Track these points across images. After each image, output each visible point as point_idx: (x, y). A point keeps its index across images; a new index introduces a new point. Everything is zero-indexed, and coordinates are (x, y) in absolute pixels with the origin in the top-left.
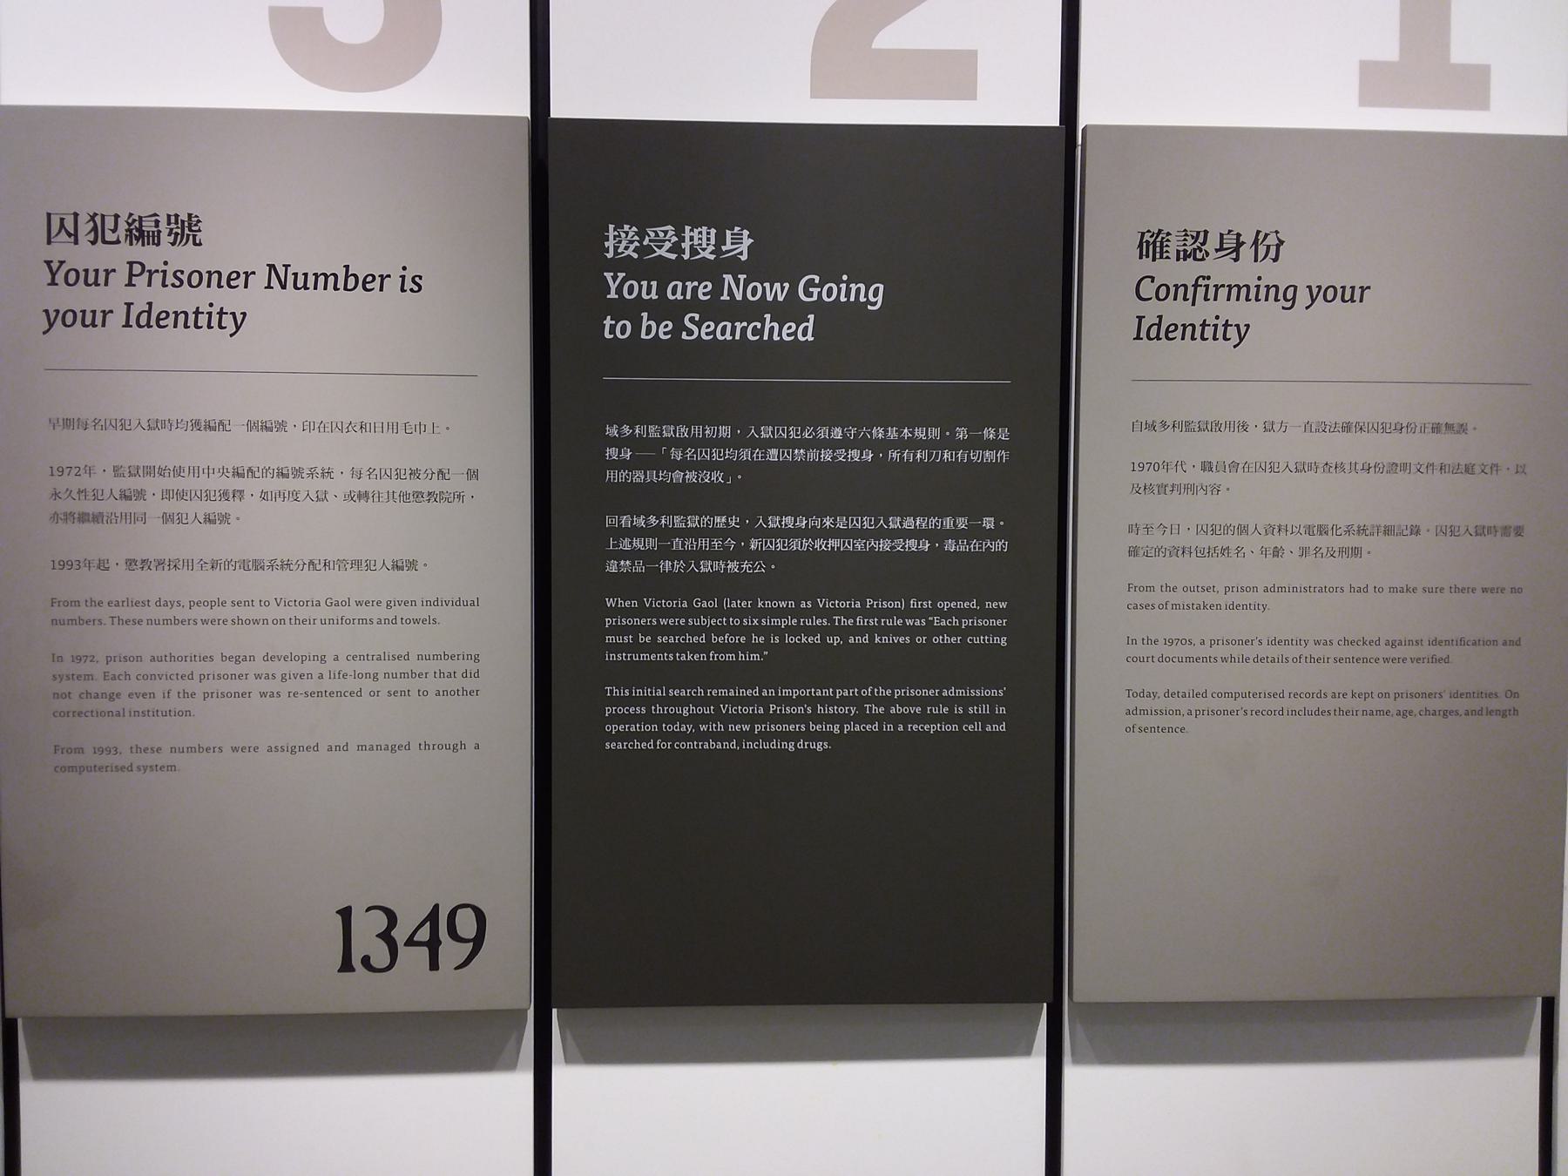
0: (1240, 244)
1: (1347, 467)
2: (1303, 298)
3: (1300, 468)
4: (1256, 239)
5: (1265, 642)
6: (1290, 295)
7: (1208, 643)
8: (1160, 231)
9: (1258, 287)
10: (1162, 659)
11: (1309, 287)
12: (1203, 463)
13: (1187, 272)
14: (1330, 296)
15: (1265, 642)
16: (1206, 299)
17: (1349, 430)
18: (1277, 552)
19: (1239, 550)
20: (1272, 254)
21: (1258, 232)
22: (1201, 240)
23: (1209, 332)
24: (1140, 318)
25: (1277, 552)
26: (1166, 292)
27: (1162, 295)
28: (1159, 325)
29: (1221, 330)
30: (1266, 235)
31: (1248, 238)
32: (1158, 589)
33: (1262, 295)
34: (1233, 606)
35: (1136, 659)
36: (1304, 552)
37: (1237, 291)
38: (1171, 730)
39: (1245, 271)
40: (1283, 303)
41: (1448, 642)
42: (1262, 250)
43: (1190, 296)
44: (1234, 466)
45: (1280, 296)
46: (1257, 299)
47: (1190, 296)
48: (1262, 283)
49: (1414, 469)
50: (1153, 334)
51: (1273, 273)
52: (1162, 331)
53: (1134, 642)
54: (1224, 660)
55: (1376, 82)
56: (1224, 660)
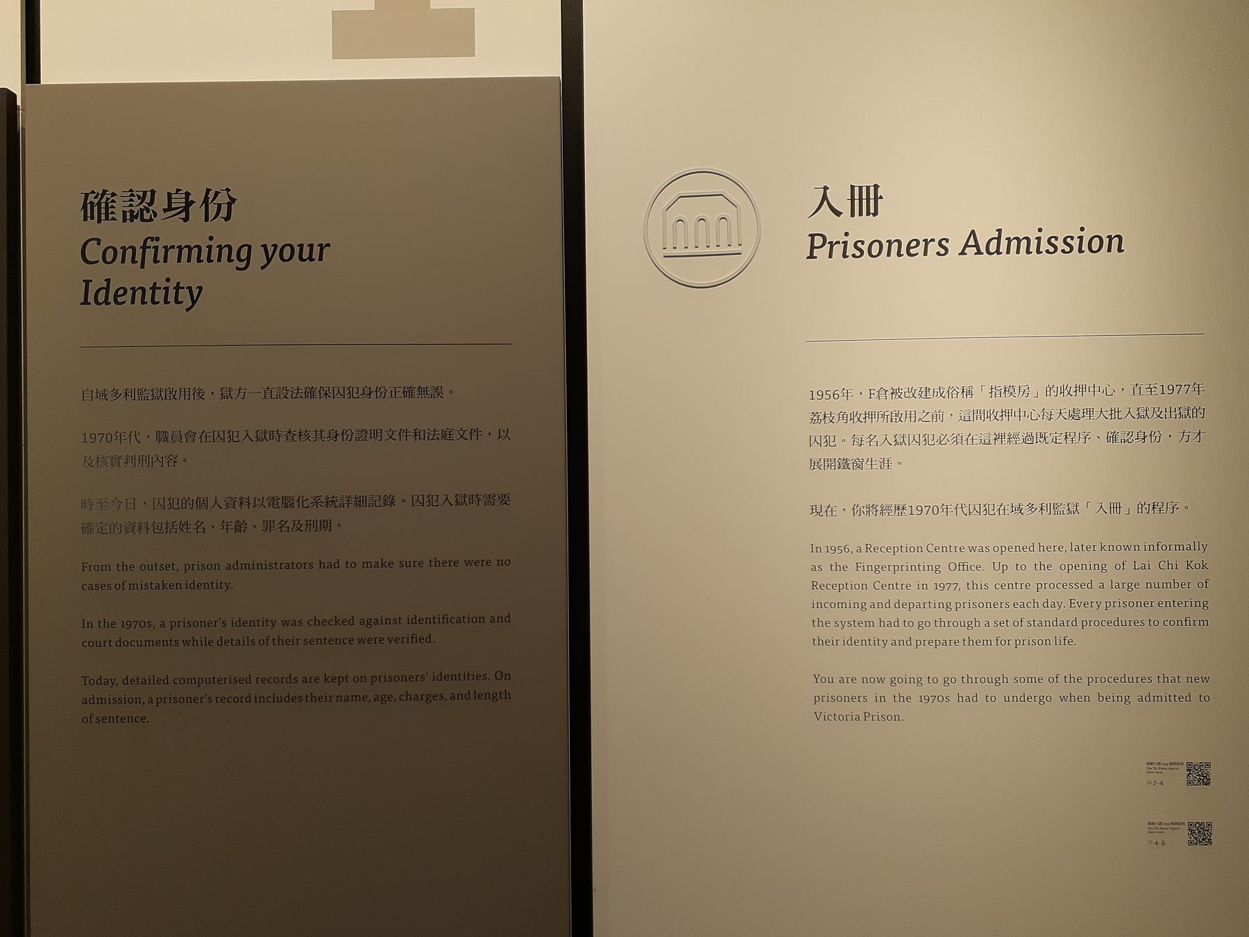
0: (189, 203)
1: (312, 435)
2: (258, 257)
3: (262, 436)
4: (206, 198)
5: (229, 623)
6: (244, 255)
7: (168, 625)
8: (105, 192)
9: (210, 247)
10: (120, 643)
11: (265, 246)
12: (158, 433)
13: (135, 233)
14: (287, 255)
15: (229, 623)
16: (156, 261)
17: (313, 396)
18: (239, 527)
19: (199, 525)
20: (224, 213)
21: (208, 191)
22: (148, 199)
23: (160, 295)
24: (87, 282)
25: (239, 527)
26: (113, 255)
27: (109, 259)
28: (107, 289)
29: (172, 293)
30: (217, 193)
31: (197, 197)
32: (114, 568)
33: (214, 256)
34: (195, 586)
35: (92, 644)
36: (268, 526)
37: (188, 252)
38: (131, 719)
39: (196, 231)
40: (236, 263)
41: (430, 620)
42: (213, 209)
43: (138, 258)
44: (191, 435)
45: (234, 256)
46: (209, 260)
47: (138, 258)
48: (214, 244)
49: (385, 436)
50: (101, 298)
51: (223, 233)
52: (110, 296)
53: (90, 625)
54: (186, 643)
55: (349, 34)
56: (186, 643)
